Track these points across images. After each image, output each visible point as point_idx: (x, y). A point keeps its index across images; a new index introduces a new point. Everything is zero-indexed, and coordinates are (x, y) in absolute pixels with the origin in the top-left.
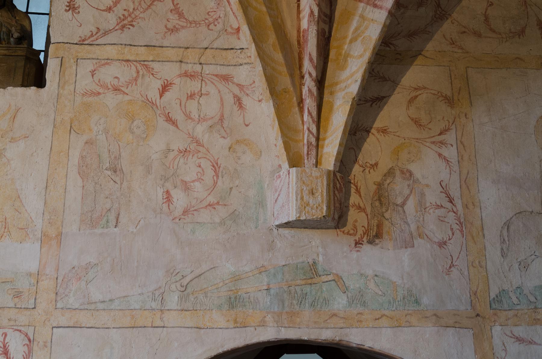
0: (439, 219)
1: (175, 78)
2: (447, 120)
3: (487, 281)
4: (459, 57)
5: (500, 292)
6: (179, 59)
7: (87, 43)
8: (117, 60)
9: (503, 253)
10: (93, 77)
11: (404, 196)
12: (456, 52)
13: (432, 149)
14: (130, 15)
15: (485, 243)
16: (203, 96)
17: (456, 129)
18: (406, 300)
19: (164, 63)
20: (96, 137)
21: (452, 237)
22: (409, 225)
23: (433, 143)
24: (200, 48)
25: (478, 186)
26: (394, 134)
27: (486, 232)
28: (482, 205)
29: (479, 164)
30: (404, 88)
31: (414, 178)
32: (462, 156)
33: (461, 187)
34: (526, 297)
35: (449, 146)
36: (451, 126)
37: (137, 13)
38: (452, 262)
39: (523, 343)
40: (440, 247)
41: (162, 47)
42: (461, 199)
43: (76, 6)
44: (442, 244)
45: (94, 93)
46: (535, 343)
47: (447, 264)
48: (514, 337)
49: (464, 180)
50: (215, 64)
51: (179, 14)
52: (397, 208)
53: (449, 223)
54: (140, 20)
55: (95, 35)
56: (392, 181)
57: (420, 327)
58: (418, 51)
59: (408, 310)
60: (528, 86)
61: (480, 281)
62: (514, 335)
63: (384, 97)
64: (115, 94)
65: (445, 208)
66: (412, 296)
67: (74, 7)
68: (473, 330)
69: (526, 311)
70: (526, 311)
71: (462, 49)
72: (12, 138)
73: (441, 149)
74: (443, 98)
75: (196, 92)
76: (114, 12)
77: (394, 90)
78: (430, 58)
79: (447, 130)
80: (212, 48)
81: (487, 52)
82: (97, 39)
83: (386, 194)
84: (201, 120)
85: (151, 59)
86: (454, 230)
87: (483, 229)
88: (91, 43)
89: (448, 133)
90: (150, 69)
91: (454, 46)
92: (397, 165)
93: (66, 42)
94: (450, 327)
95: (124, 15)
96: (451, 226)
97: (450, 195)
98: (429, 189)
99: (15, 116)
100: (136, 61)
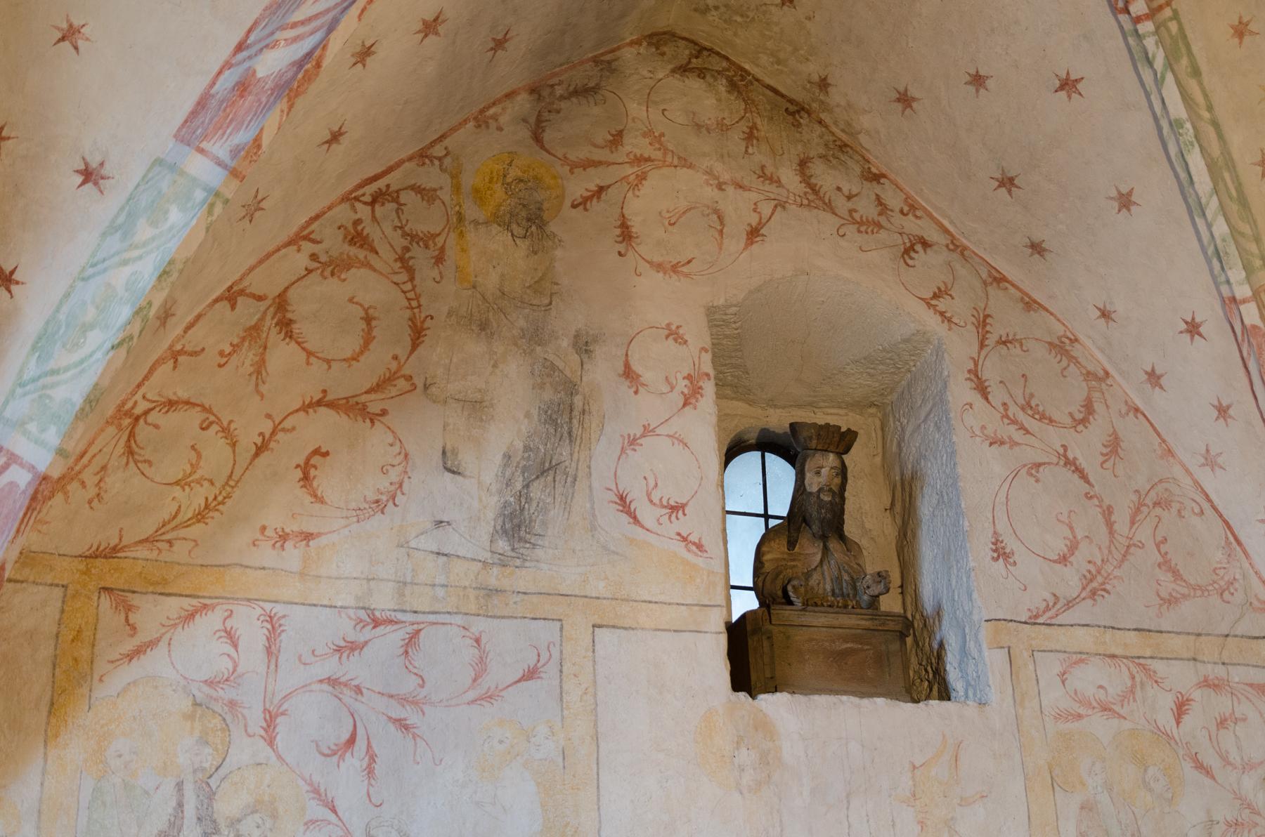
1: (1192, 691)
6: (1191, 655)
7: (1042, 622)
8: (1096, 654)
10: (1064, 685)
14: (1099, 572)
16: (1239, 723)
19: (1170, 661)
20: (1095, 797)
24: (1218, 636)
37: (1109, 568)
41: (1161, 632)
43: (1007, 551)
45: (1072, 715)
50: (1245, 665)
51: (1174, 572)
54: (1115, 582)
55: (1053, 606)
64: (1105, 717)
67: (1005, 553)
72: (962, 799)
75: (1227, 715)
76: (1072, 564)
80: (1236, 636)
82: (1057, 615)
84: (1246, 767)
85: (1148, 654)
88: (1048, 622)
90: (1152, 673)
93: (1009, 618)
95: (1089, 572)
99: (956, 757)
100: (1126, 657)
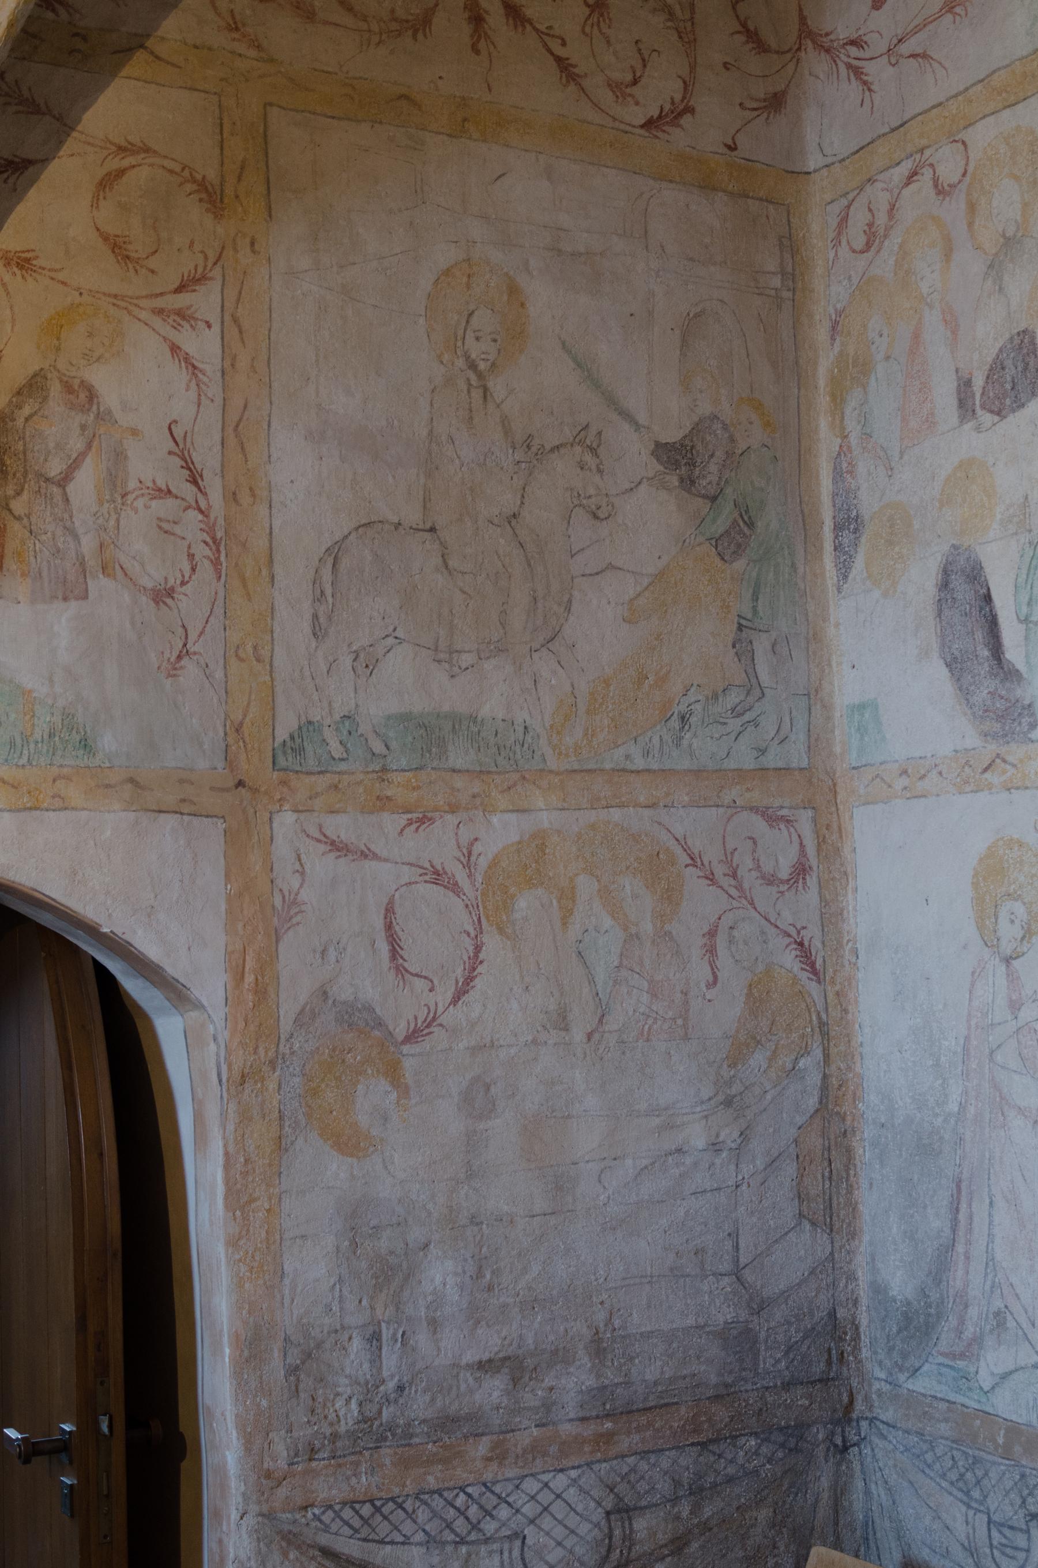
0: (160, 527)
2: (202, 252)
3: (270, 699)
4: (248, 72)
5: (300, 728)
9: (317, 628)
11: (69, 457)
12: (240, 55)
13: (154, 330)
15: (273, 598)
17: (224, 281)
18: (57, 739)
21: (190, 577)
22: (76, 537)
23: (159, 312)
25: (269, 444)
26: (53, 274)
27: (278, 570)
28: (274, 495)
29: (275, 385)
30: (89, 144)
31: (98, 409)
32: (234, 358)
33: (223, 444)
34: (364, 743)
35: (201, 325)
36: (211, 270)
38: (185, 645)
39: (346, 855)
40: (157, 603)
42: (223, 476)
44: (163, 595)
46: (376, 857)
47: (171, 648)
48: (326, 840)
49: (234, 424)
52: (47, 489)
53: (184, 538)
56: (40, 409)
57: (90, 810)
58: (136, 35)
59: (61, 766)
60: (422, 180)
61: (253, 697)
62: (325, 836)
63: (29, 163)
65: (177, 497)
66: (72, 729)
68: (225, 822)
69: (362, 776)
70: (362, 776)
71: (259, 47)
73: (177, 332)
74: (195, 187)
77: (61, 143)
78: (168, 63)
79: (199, 280)
81: (326, 68)
83: (20, 446)
86: (197, 558)
87: (271, 561)
89: (202, 289)
91: (236, 35)
92: (55, 367)
94: (168, 812)
96: (189, 547)
97: (193, 463)
98: (139, 440)
